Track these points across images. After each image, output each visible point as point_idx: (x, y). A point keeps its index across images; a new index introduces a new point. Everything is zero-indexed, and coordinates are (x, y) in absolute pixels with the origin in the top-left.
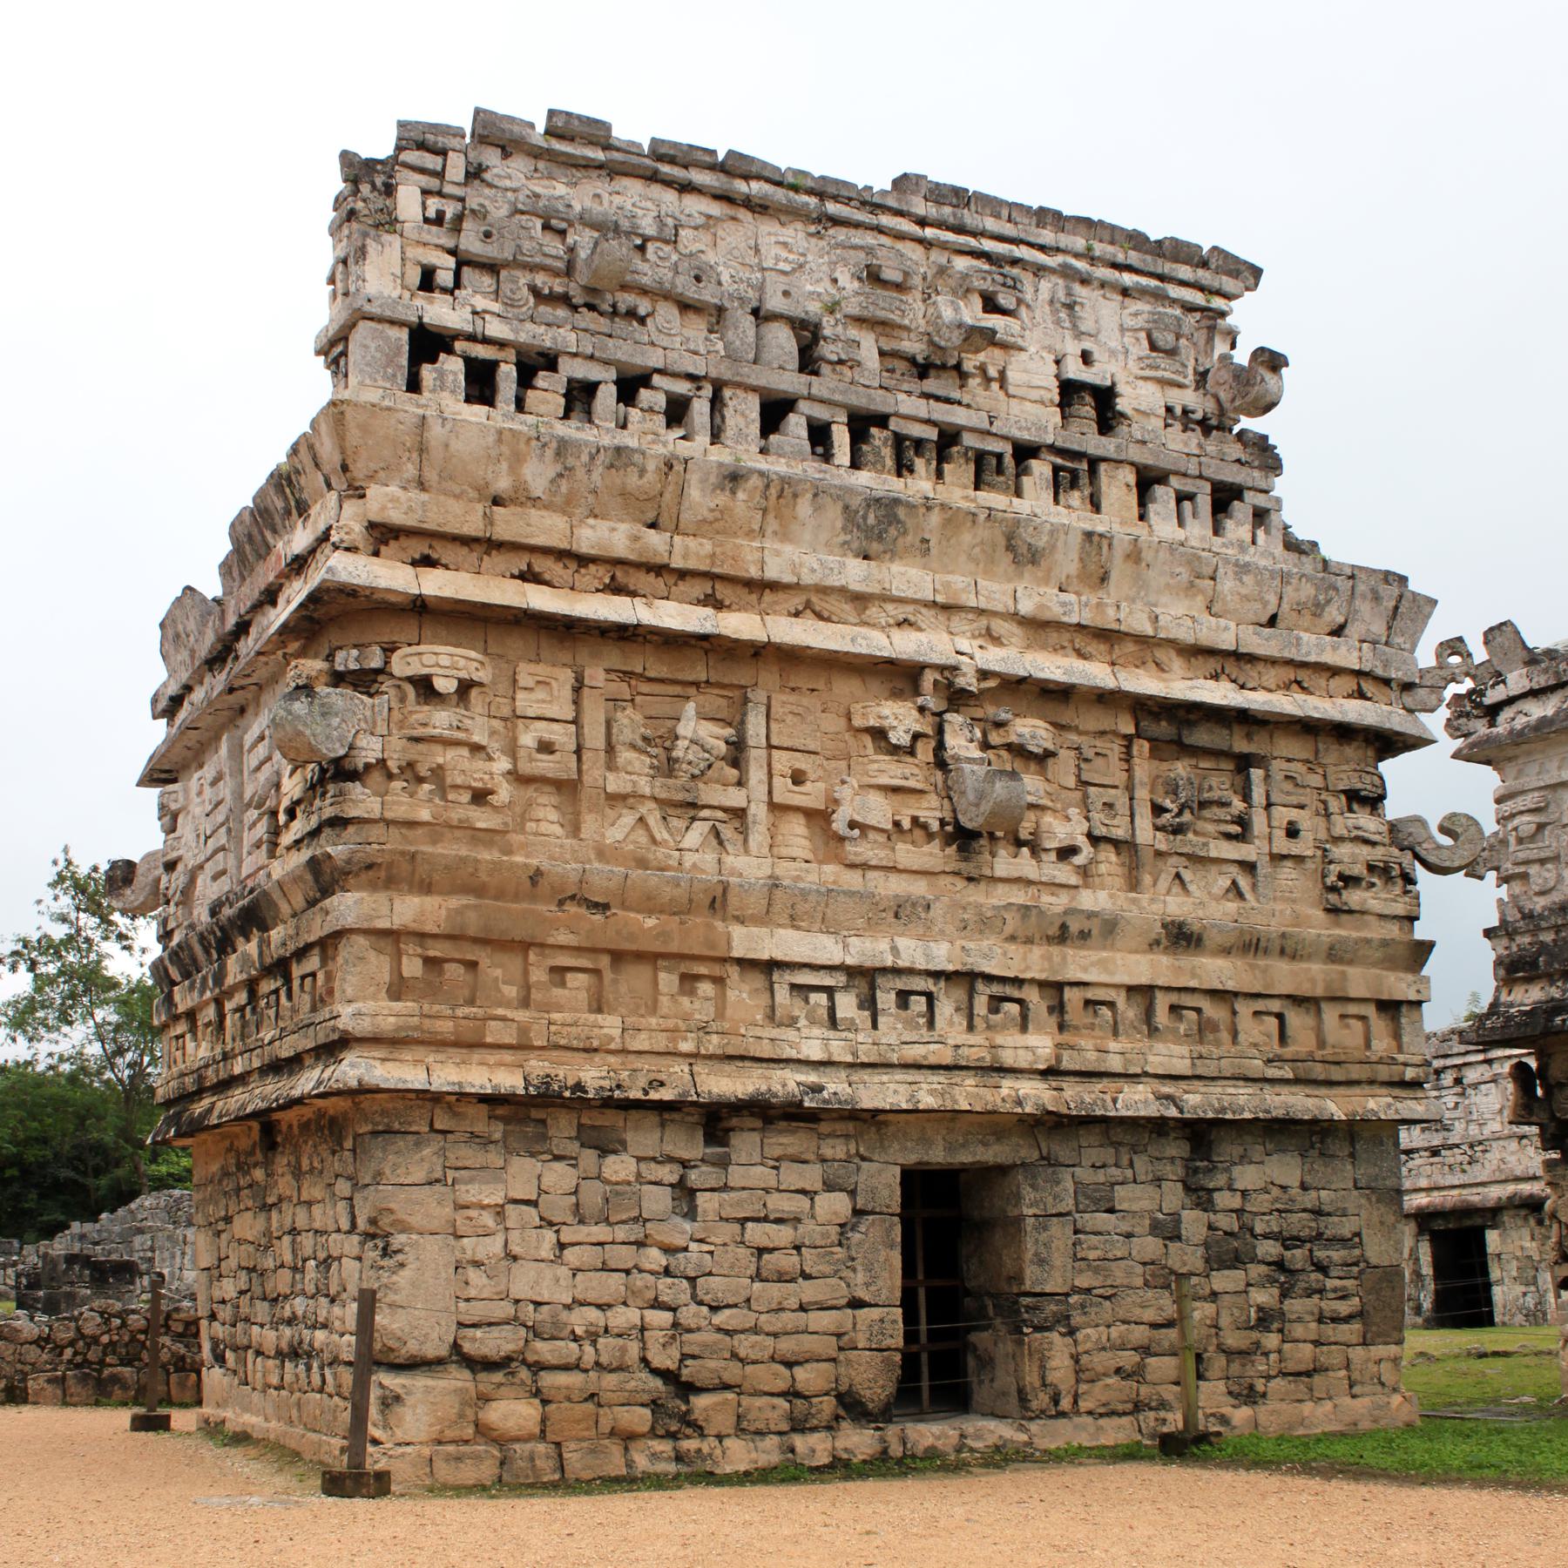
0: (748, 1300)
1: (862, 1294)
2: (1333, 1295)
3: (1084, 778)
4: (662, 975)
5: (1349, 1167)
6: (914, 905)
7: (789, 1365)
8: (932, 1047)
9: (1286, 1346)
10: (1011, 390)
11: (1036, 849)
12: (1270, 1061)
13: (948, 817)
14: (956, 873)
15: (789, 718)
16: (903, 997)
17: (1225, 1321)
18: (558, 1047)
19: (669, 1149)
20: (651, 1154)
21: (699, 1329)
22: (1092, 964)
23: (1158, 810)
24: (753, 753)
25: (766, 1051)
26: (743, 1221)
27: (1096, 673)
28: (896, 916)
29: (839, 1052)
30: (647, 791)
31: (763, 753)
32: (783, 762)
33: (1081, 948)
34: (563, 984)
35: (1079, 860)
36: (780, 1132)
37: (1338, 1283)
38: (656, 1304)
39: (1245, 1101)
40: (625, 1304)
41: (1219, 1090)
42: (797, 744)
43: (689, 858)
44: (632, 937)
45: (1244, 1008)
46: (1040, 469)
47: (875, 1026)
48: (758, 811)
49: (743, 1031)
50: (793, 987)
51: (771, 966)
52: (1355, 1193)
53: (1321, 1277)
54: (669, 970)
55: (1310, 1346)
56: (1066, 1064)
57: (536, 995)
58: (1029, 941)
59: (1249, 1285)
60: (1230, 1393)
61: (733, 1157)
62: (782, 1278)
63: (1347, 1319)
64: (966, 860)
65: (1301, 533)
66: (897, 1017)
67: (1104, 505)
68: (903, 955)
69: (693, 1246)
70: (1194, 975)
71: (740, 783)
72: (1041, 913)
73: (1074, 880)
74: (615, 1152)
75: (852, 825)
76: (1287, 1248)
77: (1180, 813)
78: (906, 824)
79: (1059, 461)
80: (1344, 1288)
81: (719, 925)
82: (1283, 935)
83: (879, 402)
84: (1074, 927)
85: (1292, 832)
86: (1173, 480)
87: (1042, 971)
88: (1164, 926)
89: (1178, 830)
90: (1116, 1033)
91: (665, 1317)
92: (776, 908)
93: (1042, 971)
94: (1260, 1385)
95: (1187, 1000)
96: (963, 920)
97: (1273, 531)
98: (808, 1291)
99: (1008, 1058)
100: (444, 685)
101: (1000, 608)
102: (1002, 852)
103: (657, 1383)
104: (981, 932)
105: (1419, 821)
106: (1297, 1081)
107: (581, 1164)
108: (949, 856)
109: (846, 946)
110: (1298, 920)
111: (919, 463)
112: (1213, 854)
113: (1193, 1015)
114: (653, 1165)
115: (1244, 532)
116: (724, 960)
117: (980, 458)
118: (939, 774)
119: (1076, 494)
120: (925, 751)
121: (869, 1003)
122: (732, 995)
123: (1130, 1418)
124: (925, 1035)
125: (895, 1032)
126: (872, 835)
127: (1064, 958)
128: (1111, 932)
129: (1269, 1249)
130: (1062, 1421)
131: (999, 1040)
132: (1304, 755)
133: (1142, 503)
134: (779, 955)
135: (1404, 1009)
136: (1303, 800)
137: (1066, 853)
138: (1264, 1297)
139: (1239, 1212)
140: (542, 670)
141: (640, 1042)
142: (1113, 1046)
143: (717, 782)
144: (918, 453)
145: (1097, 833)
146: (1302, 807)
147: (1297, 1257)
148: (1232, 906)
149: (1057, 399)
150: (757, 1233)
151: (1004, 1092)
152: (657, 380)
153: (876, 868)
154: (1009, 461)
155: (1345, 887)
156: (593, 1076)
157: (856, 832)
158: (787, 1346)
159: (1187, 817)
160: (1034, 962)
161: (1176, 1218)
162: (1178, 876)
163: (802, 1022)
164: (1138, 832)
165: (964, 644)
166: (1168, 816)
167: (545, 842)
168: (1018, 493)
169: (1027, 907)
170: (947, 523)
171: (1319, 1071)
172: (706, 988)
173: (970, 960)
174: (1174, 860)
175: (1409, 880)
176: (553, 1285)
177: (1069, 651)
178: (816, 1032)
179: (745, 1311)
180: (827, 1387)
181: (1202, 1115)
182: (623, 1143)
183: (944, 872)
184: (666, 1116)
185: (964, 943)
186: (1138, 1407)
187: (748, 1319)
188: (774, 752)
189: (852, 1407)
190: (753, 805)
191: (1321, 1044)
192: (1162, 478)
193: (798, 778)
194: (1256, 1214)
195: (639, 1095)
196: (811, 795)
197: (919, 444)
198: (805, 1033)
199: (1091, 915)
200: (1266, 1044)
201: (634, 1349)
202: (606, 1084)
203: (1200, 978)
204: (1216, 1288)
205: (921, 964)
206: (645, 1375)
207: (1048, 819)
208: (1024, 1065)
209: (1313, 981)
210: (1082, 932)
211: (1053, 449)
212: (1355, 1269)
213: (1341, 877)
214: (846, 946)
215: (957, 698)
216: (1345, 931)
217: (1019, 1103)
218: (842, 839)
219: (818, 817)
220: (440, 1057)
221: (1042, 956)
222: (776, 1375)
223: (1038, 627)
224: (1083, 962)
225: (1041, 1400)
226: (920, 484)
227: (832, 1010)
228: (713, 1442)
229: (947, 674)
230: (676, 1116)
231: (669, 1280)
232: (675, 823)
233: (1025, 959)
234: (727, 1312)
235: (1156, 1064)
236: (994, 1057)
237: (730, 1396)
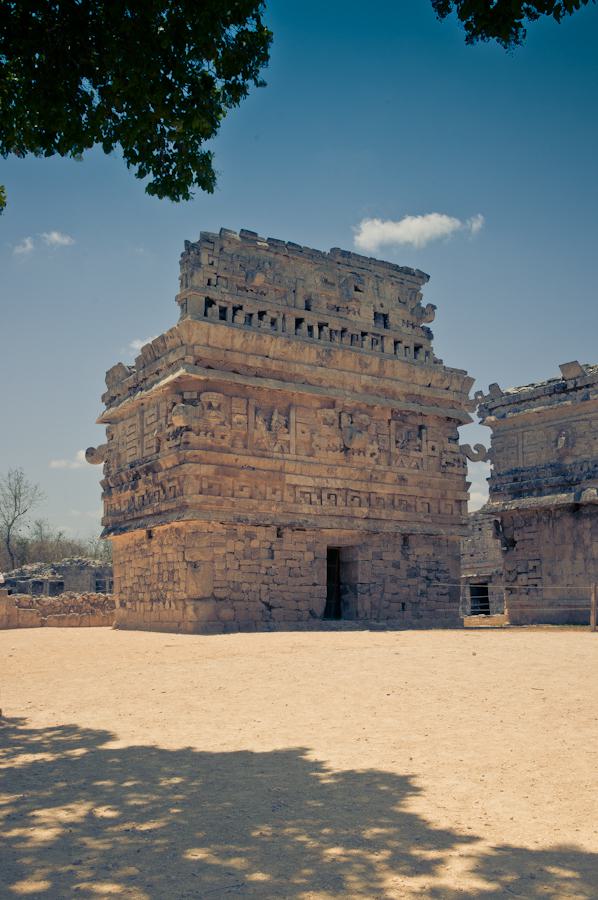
1: (316, 582)
7: (297, 601)
23: (397, 442)
26: (286, 560)
35: (375, 457)
46: (368, 338)
50: (301, 492)
51: (295, 486)
56: (371, 516)
62: (296, 576)
63: (445, 595)
65: (438, 356)
71: (288, 433)
83: (326, 320)
85: (433, 449)
94: (421, 613)
98: (302, 580)
99: (356, 514)
100: (215, 405)
103: (263, 606)
105: (468, 446)
115: (423, 358)
121: (320, 497)
129: (424, 573)
133: (395, 349)
138: (423, 587)
142: (383, 511)
147: (431, 576)
150: (290, 563)
152: (268, 313)
158: (297, 596)
168: (362, 347)
175: (465, 464)
176: (237, 577)
197: (336, 331)
206: (260, 603)
211: (373, 334)
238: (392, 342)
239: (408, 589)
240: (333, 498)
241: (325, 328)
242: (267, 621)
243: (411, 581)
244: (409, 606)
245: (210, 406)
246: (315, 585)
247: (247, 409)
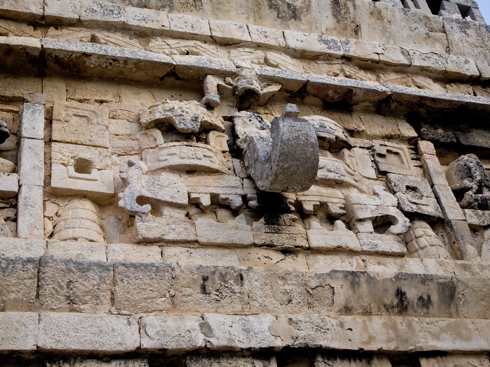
6: (223, 277)
13: (250, 193)
14: (270, 246)
22: (443, 330)
28: (204, 290)
33: (427, 315)
58: (367, 312)
64: (278, 232)
68: (217, 333)
72: (371, 279)
73: (398, 248)
75: (141, 200)
77: (479, 191)
78: (206, 201)
84: (412, 294)
87: (389, 341)
92: (48, 289)
93: (389, 341)
96: (286, 292)
102: (315, 223)
104: (310, 305)
108: (259, 229)
109: (142, 327)
118: (237, 162)
126: (167, 211)
127: (410, 326)
128: (452, 296)
137: (382, 224)
153: (175, 243)
157: (147, 207)
164: (447, 210)
166: (470, 192)
173: (302, 334)
183: (255, 245)
190: (23, 188)
193: (83, 166)
199: (425, 279)
205: (242, 342)
210: (421, 298)
214: (142, 327)
218: (132, 216)
219: (104, 202)
221: (384, 325)
224: (434, 329)
229: (229, 79)
233: (365, 329)
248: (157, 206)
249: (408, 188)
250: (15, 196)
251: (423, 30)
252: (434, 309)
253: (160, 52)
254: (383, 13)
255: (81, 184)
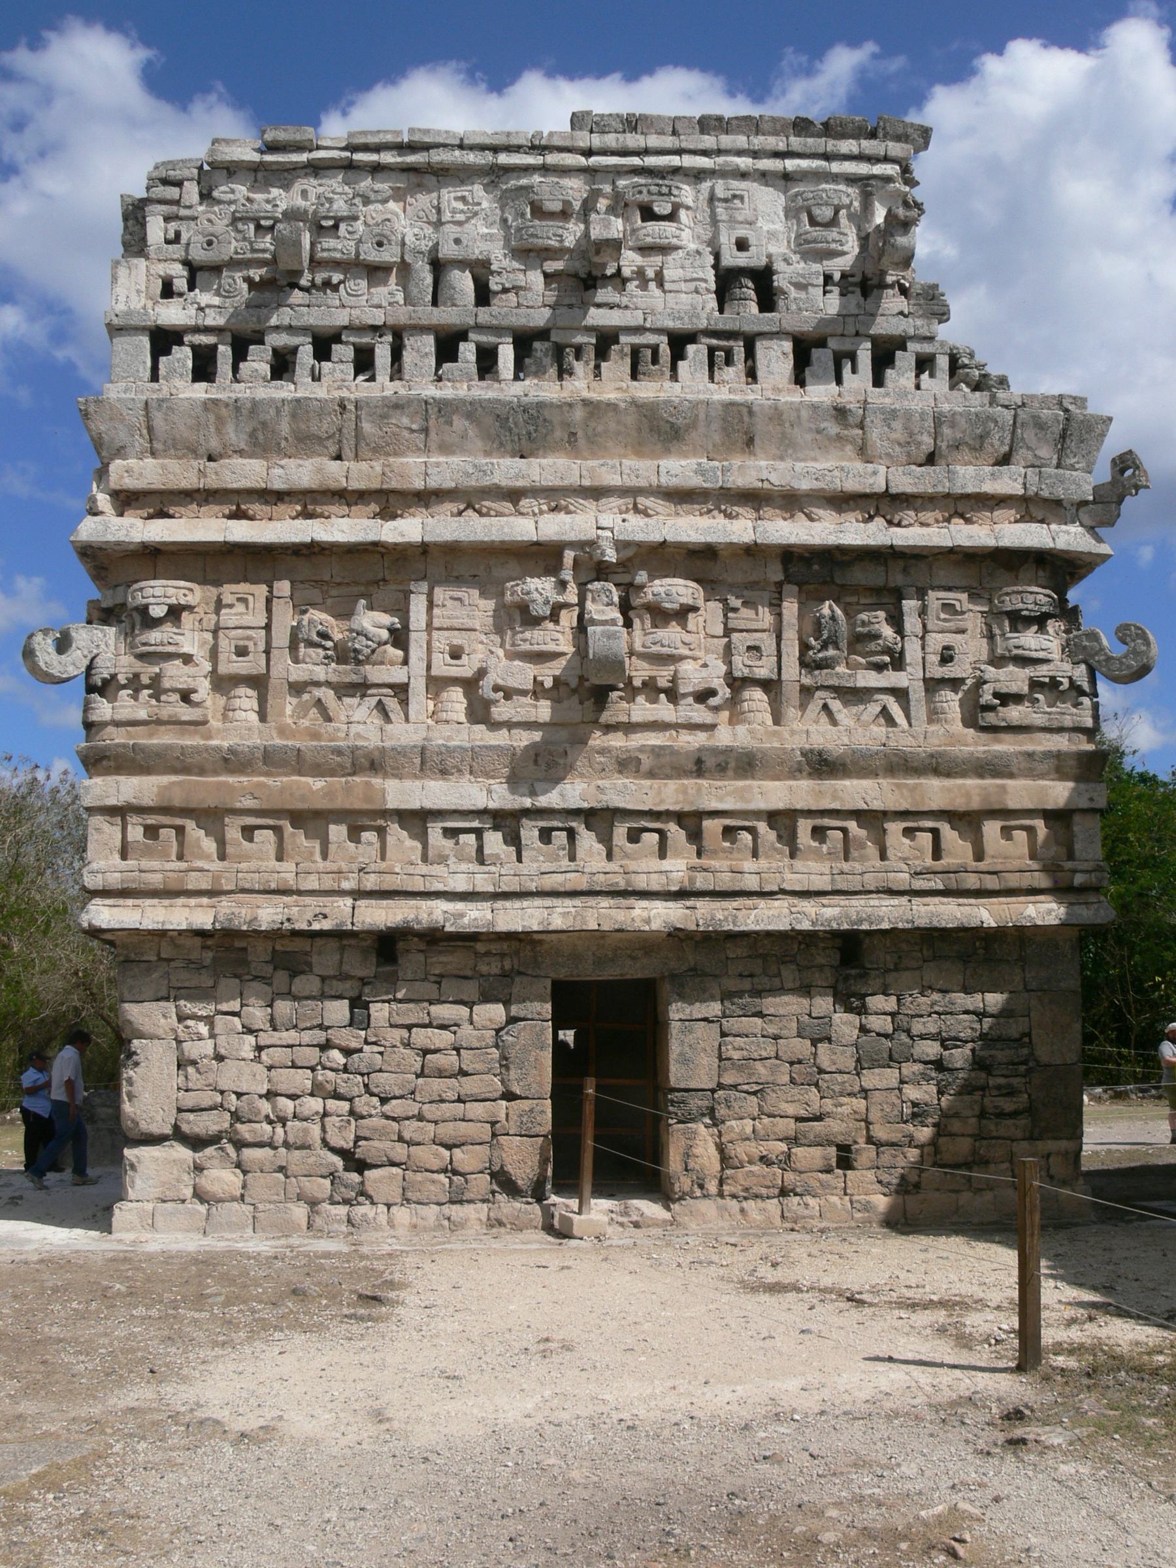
0: (413, 1093)
2: (995, 1093)
3: (730, 625)
4: (333, 828)
5: (1018, 970)
7: (449, 1147)
8: (568, 875)
9: (942, 1140)
10: (667, 286)
11: (673, 695)
12: (916, 874)
15: (449, 603)
16: (546, 835)
17: (874, 1115)
18: (244, 891)
19: (346, 968)
20: (332, 973)
21: (371, 1116)
22: (728, 794)
23: (805, 647)
24: (413, 636)
25: (418, 885)
26: (409, 1027)
27: (741, 529)
29: (483, 883)
30: (322, 677)
31: (424, 635)
32: (441, 641)
34: (251, 840)
35: (713, 701)
36: (440, 952)
37: (1001, 1081)
38: (337, 1096)
39: (888, 913)
40: (312, 1095)
41: (862, 902)
42: (456, 623)
43: (355, 729)
44: (303, 798)
45: (894, 828)
47: (519, 860)
48: (418, 686)
49: (397, 870)
52: (1026, 995)
53: (984, 1075)
54: (336, 822)
55: (969, 1140)
57: (230, 850)
58: (668, 777)
59: (902, 1082)
60: (880, 1182)
61: (400, 974)
62: (441, 1074)
63: (1014, 1114)
66: (538, 850)
67: (761, 373)
69: (366, 1048)
70: (835, 797)
74: (303, 972)
75: (497, 688)
76: (946, 1048)
79: (714, 342)
80: (1010, 1086)
81: (377, 781)
82: (932, 756)
84: (710, 762)
86: (833, 343)
87: (677, 803)
88: (803, 754)
89: (821, 665)
90: (755, 854)
91: (345, 1106)
93: (677, 803)
95: (827, 822)
97: (938, 374)
98: (469, 1086)
99: (641, 883)
101: (643, 483)
102: (640, 699)
104: (620, 772)
106: (946, 893)
107: (276, 982)
110: (953, 739)
111: (579, 367)
112: (861, 683)
113: (840, 834)
114: (334, 982)
116: (385, 813)
117: (635, 352)
119: (731, 370)
120: (568, 619)
121: (514, 839)
122: (390, 840)
123: (775, 1201)
124: (565, 863)
125: (540, 863)
127: (699, 790)
130: (707, 1202)
131: (632, 865)
132: (964, 583)
134: (428, 804)
135: (1077, 818)
136: (961, 624)
137: (703, 696)
138: (912, 1093)
139: (893, 1015)
140: (243, 587)
141: (312, 883)
142: (749, 865)
143: (382, 663)
144: (578, 357)
145: (737, 674)
146: (963, 631)
148: (880, 731)
149: (713, 287)
150: (421, 1037)
151: (636, 912)
154: (665, 351)
155: (1003, 704)
156: (268, 914)
157: (501, 694)
158: (448, 1131)
159: (831, 652)
160: (670, 794)
161: (826, 1019)
162: (825, 707)
163: (452, 860)
165: (606, 520)
167: (241, 724)
168: (674, 377)
169: (661, 747)
170: (591, 414)
171: (972, 881)
172: (369, 836)
174: (819, 694)
176: (254, 1080)
177: (716, 513)
178: (464, 867)
179: (410, 1102)
180: (480, 1167)
181: (835, 926)
182: (310, 965)
184: (345, 942)
185: (600, 783)
186: (784, 1192)
187: (414, 1109)
188: (435, 634)
189: (504, 1182)
191: (979, 856)
192: (822, 343)
194: (913, 1016)
195: (304, 926)
196: (465, 668)
198: (453, 867)
200: (917, 858)
201: (316, 1130)
202: (279, 918)
203: (842, 799)
204: (866, 1085)
207: (687, 667)
208: (655, 887)
209: (968, 795)
212: (1023, 1068)
213: (996, 695)
214: (489, 792)
215: (602, 571)
216: (1006, 746)
217: (648, 921)
219: (470, 685)
220: (155, 901)
222: (436, 1155)
223: (681, 497)
225: (684, 1183)
226: (580, 384)
227: (480, 849)
228: (382, 1208)
230: (353, 942)
231: (346, 1076)
232: (347, 700)
233: (659, 792)
234: (394, 1102)
235: (793, 881)
236: (628, 883)
237: (394, 1170)
238: (788, 346)
239: (860, 1104)
240: (560, 838)
241: (537, 345)
242: (347, 1202)
243: (871, 1078)
244: (865, 1154)
245: (144, 610)
246: (509, 1096)
247: (269, 610)
248: (509, 693)
249: (749, 648)
250: (407, 685)
251: (833, 429)
252: (730, 773)
253: (522, 527)
254: (785, 417)
255: (454, 672)
